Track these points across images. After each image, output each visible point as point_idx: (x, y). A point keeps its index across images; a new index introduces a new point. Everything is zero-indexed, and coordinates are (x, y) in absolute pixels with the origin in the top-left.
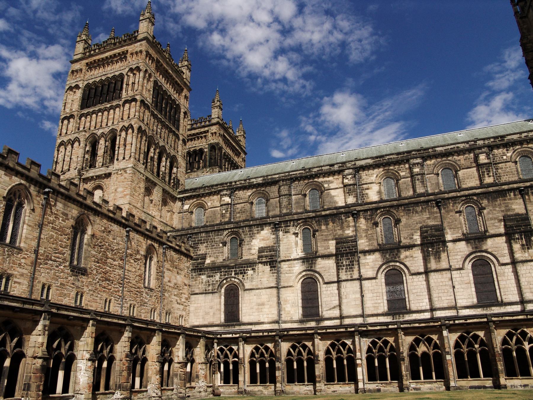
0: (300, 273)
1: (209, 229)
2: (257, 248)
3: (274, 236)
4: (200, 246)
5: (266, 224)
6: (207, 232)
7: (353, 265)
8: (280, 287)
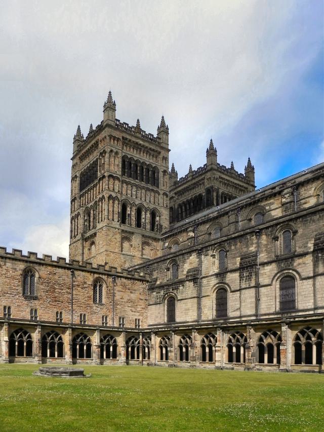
0: (215, 285)
1: (158, 260)
2: (187, 270)
3: (198, 260)
4: (154, 273)
5: (193, 251)
6: (157, 262)
7: (251, 276)
8: (203, 294)
